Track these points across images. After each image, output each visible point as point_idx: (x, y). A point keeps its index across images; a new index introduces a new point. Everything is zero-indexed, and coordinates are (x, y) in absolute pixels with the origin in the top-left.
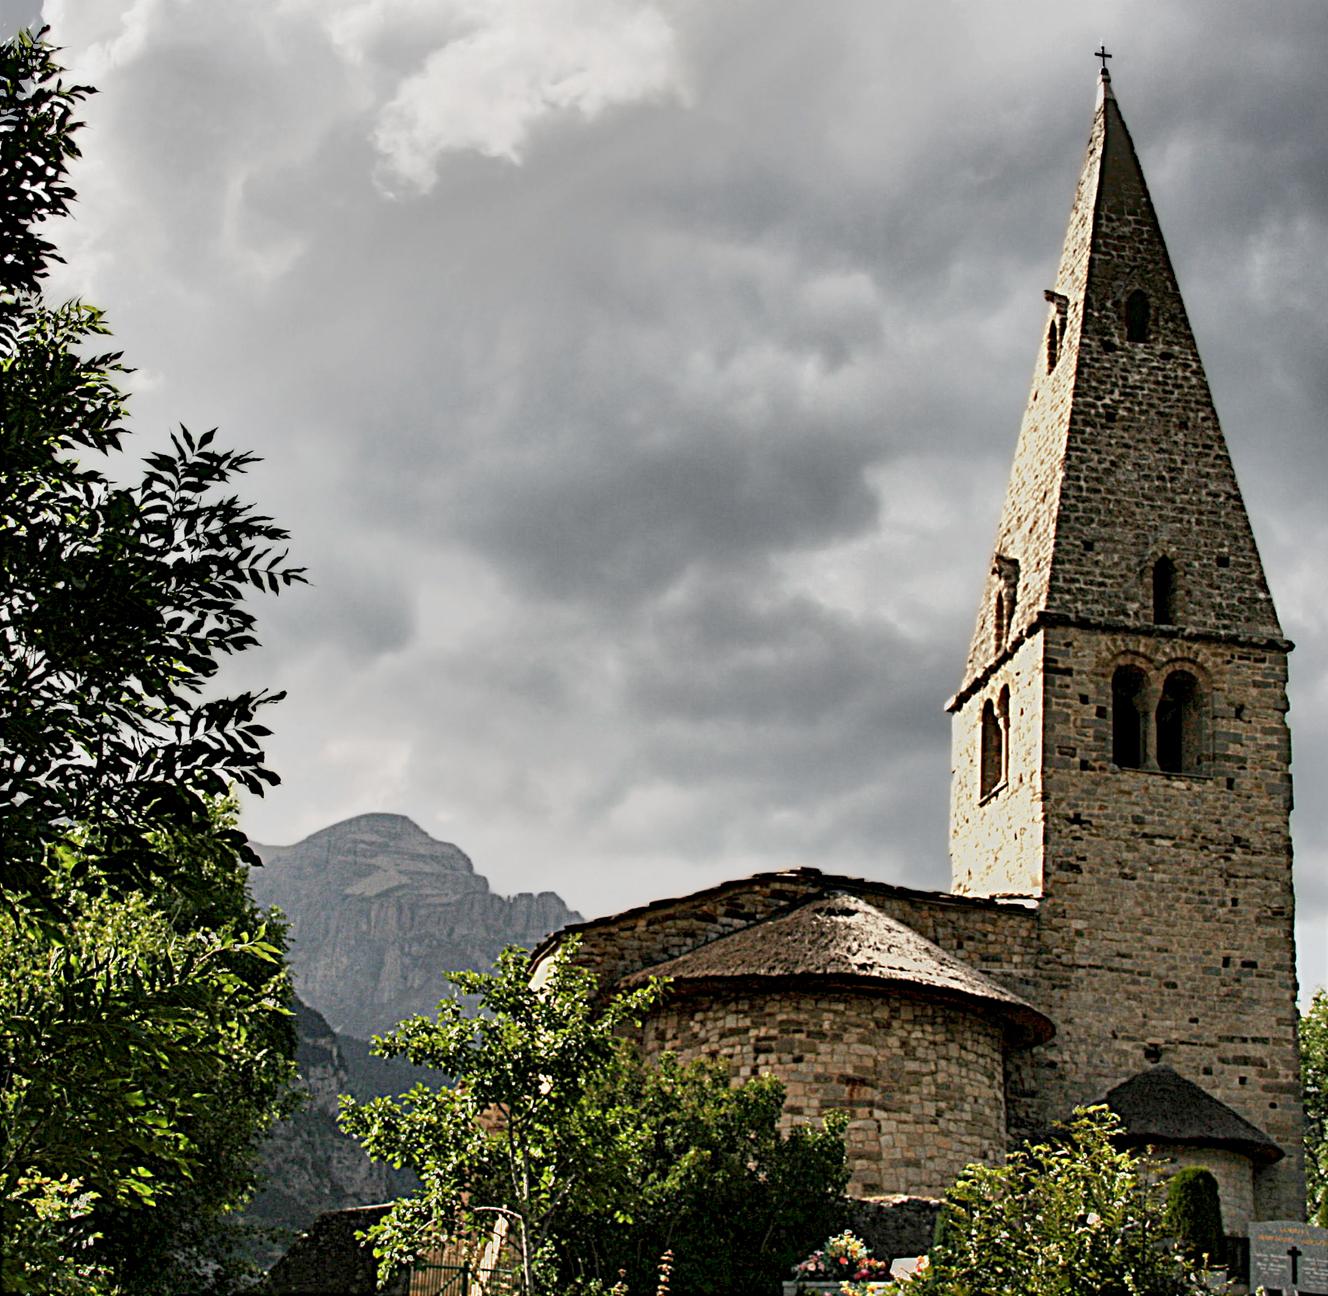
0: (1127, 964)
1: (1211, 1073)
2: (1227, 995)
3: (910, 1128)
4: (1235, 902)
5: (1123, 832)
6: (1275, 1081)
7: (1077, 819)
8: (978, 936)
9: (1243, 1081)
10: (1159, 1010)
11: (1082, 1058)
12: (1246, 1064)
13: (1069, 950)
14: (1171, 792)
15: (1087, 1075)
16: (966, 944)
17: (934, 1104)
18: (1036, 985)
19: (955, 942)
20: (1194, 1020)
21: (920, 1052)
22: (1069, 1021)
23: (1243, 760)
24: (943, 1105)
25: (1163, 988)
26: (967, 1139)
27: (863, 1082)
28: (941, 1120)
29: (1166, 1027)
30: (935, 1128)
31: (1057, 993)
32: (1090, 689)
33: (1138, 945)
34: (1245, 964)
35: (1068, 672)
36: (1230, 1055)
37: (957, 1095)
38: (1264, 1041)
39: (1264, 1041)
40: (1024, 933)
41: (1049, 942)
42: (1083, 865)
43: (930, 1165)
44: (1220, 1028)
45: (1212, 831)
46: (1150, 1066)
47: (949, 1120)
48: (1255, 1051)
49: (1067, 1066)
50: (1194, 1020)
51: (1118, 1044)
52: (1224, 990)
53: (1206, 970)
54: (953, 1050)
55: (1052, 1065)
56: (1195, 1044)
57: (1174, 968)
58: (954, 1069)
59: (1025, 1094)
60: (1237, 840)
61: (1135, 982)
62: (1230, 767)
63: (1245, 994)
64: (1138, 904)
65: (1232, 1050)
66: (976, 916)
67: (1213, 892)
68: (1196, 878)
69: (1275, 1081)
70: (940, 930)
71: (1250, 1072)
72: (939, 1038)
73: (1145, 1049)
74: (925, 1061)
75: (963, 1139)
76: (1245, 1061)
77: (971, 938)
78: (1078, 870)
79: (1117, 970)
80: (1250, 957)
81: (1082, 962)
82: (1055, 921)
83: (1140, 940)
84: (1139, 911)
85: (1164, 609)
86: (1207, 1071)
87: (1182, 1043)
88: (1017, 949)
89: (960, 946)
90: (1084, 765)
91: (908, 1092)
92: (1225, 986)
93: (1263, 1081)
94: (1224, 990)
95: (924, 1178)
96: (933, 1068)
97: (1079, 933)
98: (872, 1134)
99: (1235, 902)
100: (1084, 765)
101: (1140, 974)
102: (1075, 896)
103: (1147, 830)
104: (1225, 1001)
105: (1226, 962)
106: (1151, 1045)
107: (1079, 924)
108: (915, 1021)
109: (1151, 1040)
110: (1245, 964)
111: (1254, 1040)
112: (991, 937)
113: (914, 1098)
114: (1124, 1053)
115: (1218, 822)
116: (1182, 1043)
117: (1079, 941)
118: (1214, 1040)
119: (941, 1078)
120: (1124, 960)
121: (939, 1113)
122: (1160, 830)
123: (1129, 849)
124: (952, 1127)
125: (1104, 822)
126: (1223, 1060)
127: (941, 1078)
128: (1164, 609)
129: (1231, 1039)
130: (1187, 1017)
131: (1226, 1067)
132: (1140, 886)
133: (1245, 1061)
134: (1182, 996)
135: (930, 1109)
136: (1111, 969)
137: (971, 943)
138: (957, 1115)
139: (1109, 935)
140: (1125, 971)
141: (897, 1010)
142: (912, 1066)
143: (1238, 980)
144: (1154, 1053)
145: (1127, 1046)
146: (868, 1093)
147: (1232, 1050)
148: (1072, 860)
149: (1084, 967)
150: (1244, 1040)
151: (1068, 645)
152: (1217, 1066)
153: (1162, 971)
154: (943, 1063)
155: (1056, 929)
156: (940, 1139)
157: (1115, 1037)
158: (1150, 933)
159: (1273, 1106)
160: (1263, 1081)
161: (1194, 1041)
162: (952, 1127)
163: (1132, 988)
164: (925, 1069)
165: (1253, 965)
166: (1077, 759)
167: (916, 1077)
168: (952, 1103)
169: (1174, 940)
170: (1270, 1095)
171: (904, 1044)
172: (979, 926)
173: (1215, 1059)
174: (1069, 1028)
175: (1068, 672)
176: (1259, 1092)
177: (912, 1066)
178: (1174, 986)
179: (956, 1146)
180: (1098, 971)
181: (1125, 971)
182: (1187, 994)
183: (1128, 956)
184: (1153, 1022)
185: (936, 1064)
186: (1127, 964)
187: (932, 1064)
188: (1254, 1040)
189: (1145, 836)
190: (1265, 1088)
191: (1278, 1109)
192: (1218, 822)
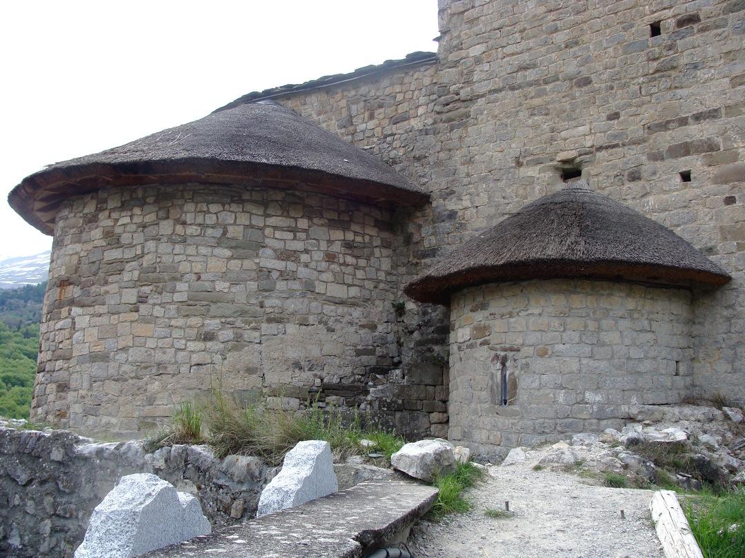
0: (531, 75)
1: (639, 178)
2: (657, 71)
3: (104, 320)
6: (731, 165)
8: (389, 101)
9: (686, 177)
10: (569, 118)
11: (484, 197)
12: (687, 153)
13: (468, 82)
16: (376, 113)
17: (135, 290)
18: (436, 133)
19: (367, 115)
20: (615, 116)
21: (125, 239)
24: (147, 289)
25: (575, 89)
28: (142, 307)
30: (135, 316)
31: (456, 134)
33: (543, 49)
36: (664, 147)
37: (166, 276)
38: (713, 114)
39: (713, 114)
40: (427, 81)
41: (445, 80)
43: (122, 356)
44: (649, 114)
46: (561, 186)
47: (154, 305)
48: (697, 132)
49: (468, 213)
50: (615, 116)
52: (655, 64)
53: (628, 48)
54: (166, 227)
55: (452, 215)
56: (616, 146)
58: (164, 247)
59: (425, 255)
61: (544, 93)
63: (684, 60)
65: (666, 139)
66: (385, 82)
69: (731, 165)
70: (354, 107)
71: (694, 163)
72: (150, 218)
73: (556, 168)
74: (131, 246)
75: (173, 322)
76: (685, 149)
77: (381, 106)
79: (520, 87)
80: (683, 9)
81: (482, 91)
82: (452, 57)
86: (635, 177)
87: (600, 149)
88: (422, 100)
91: (106, 283)
92: (655, 59)
93: (714, 171)
94: (655, 64)
95: (111, 371)
96: (139, 252)
97: (478, 61)
98: (66, 333)
101: (546, 83)
102: (473, 22)
104: (655, 79)
105: (655, 30)
106: (564, 162)
107: (476, 51)
108: (123, 207)
109: (563, 156)
110: (681, 23)
111: (698, 118)
112: (400, 97)
113: (113, 288)
114: (531, 181)
116: (600, 149)
117: (478, 69)
119: (147, 261)
120: (527, 73)
121: (142, 299)
124: (158, 311)
126: (656, 157)
127: (147, 261)
129: (664, 126)
130: (604, 116)
131: (658, 164)
133: (685, 149)
134: (599, 90)
135: (131, 296)
136: (513, 88)
137: (381, 110)
138: (166, 297)
139: (508, 50)
140: (530, 84)
142: (114, 254)
143: (670, 48)
144: (570, 171)
146: (74, 292)
147: (666, 139)
149: (483, 96)
150: (683, 122)
152: (648, 166)
153: (571, 68)
154: (151, 245)
155: (455, 64)
156: (141, 329)
157: (519, 164)
158: (556, 30)
159: (730, 200)
160: (714, 171)
161: (615, 142)
162: (158, 311)
163: (537, 101)
164: (129, 254)
165: (693, 19)
167: (118, 267)
168: (161, 285)
169: (585, 27)
170: (727, 187)
171: (108, 234)
172: (387, 91)
173: (644, 158)
174: (470, 169)
176: (711, 187)
177: (114, 254)
178: (587, 81)
179: (160, 331)
180: (499, 95)
181: (530, 84)
182: (603, 86)
183: (534, 66)
184: (563, 134)
185: (143, 248)
186: (531, 75)
187: (139, 247)
188: (698, 118)
190: (721, 179)
191: (738, 204)
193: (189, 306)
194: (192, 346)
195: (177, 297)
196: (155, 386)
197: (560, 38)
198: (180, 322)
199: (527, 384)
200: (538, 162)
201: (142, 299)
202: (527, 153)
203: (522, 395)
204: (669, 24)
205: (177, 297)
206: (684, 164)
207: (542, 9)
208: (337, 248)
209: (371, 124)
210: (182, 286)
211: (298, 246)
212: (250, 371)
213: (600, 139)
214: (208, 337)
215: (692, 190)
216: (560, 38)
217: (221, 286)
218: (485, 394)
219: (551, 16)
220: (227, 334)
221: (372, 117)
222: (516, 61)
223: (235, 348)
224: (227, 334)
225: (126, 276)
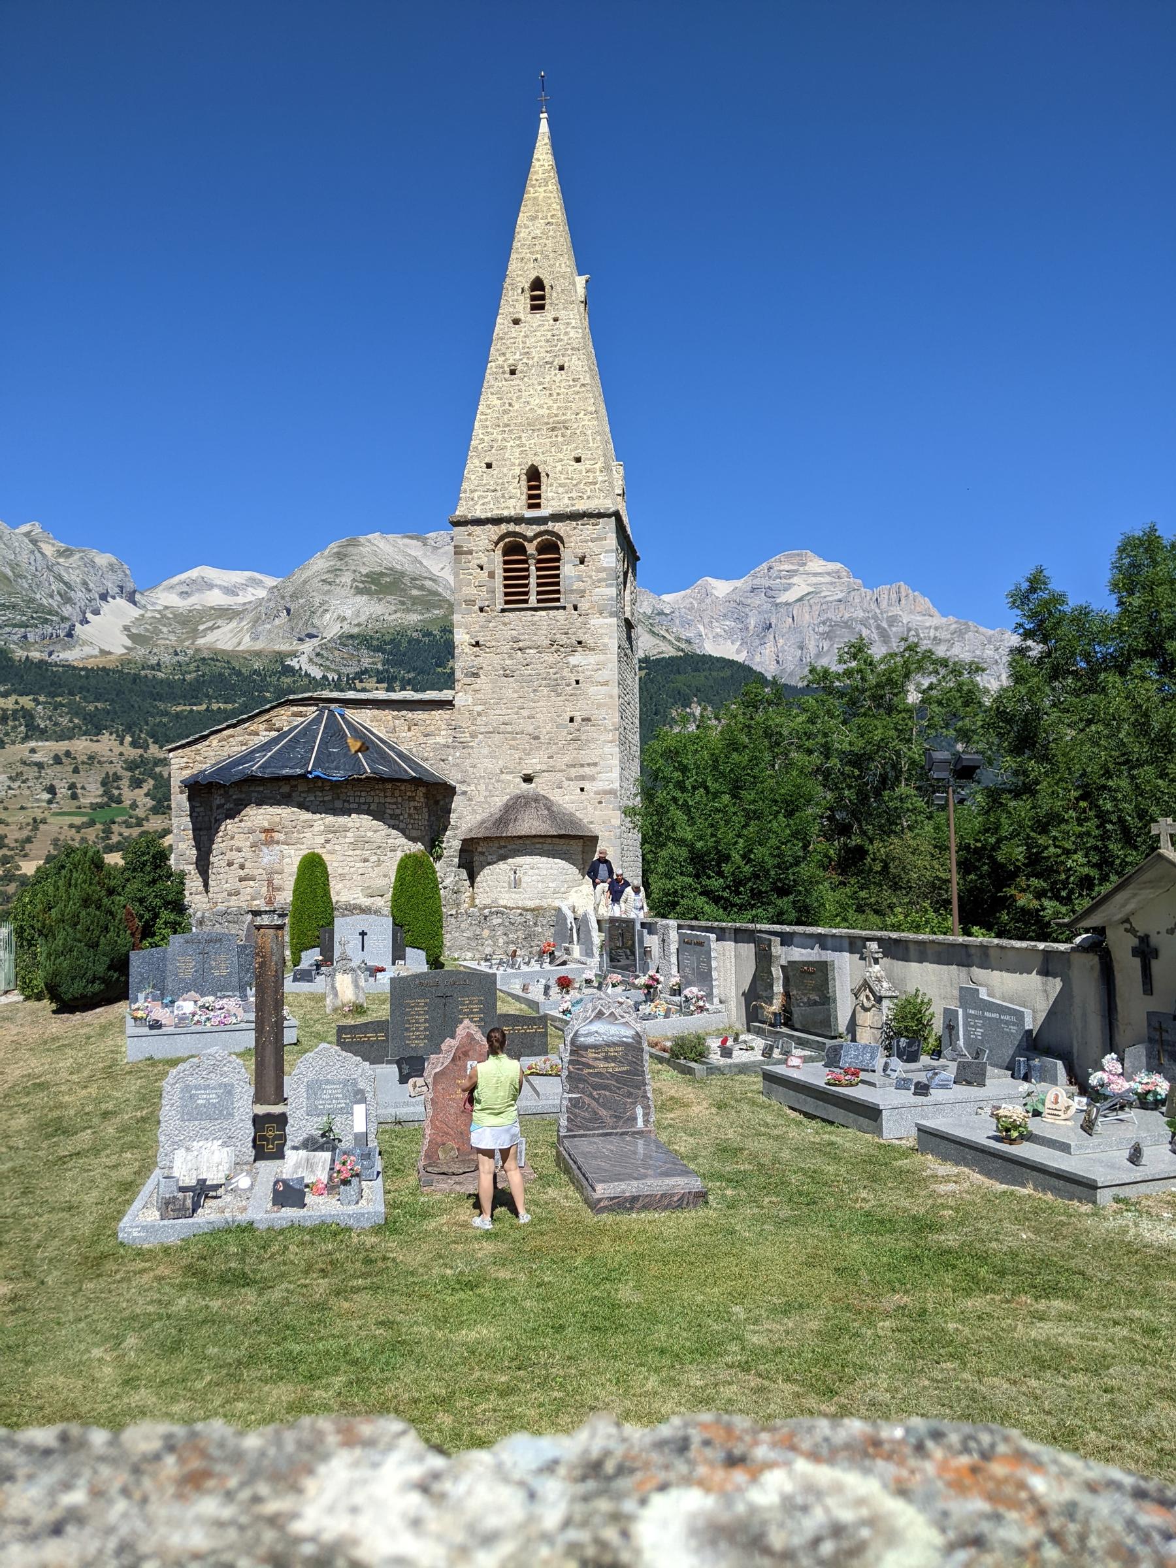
0: (509, 728)
4: (577, 682)
5: (505, 649)
7: (477, 644)
8: (421, 722)
9: (582, 790)
14: (536, 618)
15: (486, 797)
22: (474, 767)
23: (584, 591)
26: (351, 853)
27: (273, 830)
29: (532, 764)
32: (484, 560)
34: (583, 720)
35: (470, 552)
42: (481, 672)
44: (567, 759)
45: (563, 640)
46: (525, 786)
51: (503, 776)
57: (539, 727)
60: (580, 643)
61: (514, 739)
62: (574, 598)
64: (516, 692)
67: (563, 678)
68: (551, 671)
76: (582, 778)
78: (476, 675)
80: (585, 714)
83: (517, 713)
84: (516, 695)
85: (534, 501)
88: (444, 727)
89: (409, 730)
90: (481, 610)
97: (479, 714)
99: (577, 682)
100: (481, 610)
103: (521, 644)
105: (572, 720)
111: (589, 765)
113: (308, 835)
114: (509, 782)
115: (566, 634)
118: (564, 767)
121: (327, 841)
122: (527, 643)
123: (511, 657)
124: (337, 847)
125: (493, 644)
126: (569, 779)
128: (534, 501)
129: (574, 766)
132: (516, 681)
138: (341, 840)
139: (497, 712)
141: (296, 786)
144: (528, 779)
145: (510, 777)
147: (573, 772)
148: (474, 670)
150: (582, 766)
151: (469, 535)
153: (530, 729)
157: (502, 772)
159: (600, 803)
162: (337, 847)
163: (512, 742)
165: (588, 720)
166: (477, 607)
175: (470, 552)
186: (509, 728)
188: (589, 765)
189: (520, 649)
192: (566, 634)
193: (354, 845)
194: (358, 865)
195: (347, 840)
196: (340, 886)
197: (525, 713)
198: (351, 853)
199: (525, 879)
200: (512, 773)
201: (327, 841)
202: (507, 768)
203: (524, 885)
204: (578, 719)
205: (347, 840)
206: (582, 784)
207: (516, 695)
208: (412, 811)
209: (410, 734)
210: (349, 834)
211: (398, 812)
212: (385, 876)
213: (544, 767)
214: (366, 860)
215: (584, 796)
216: (525, 713)
217: (369, 834)
218: (506, 885)
219: (521, 700)
220: (375, 858)
221: (409, 730)
222: (502, 719)
223: (378, 866)
224: (375, 858)
225: (316, 829)
